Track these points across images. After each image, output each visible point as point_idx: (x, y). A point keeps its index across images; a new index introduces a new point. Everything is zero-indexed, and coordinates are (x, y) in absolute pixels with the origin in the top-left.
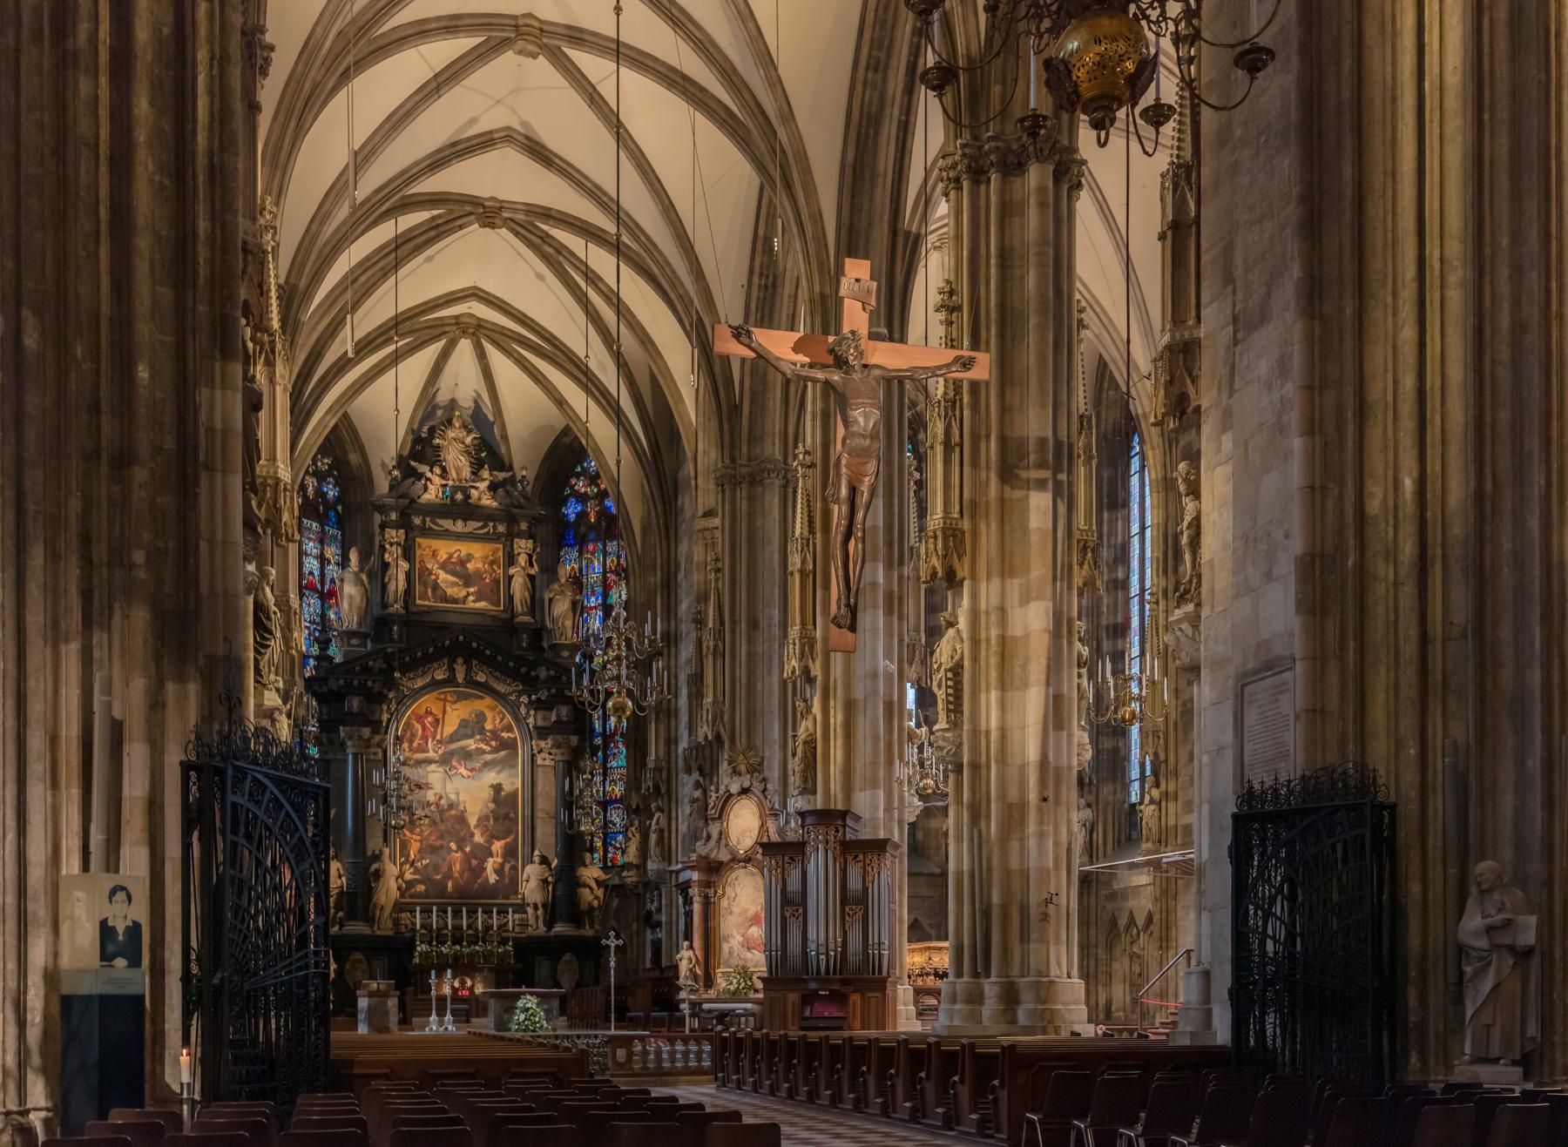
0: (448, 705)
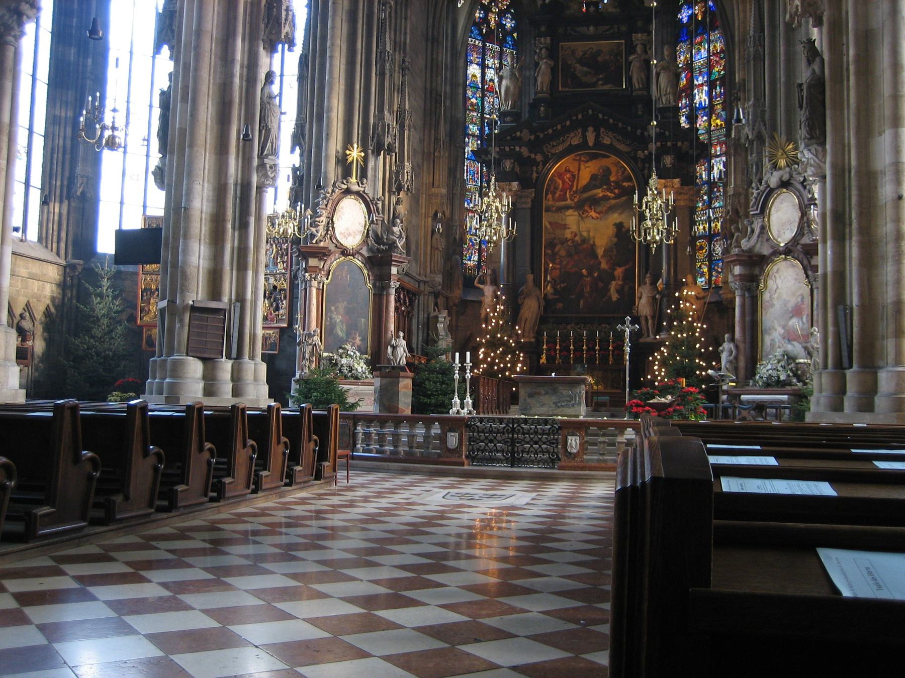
0: (582, 163)
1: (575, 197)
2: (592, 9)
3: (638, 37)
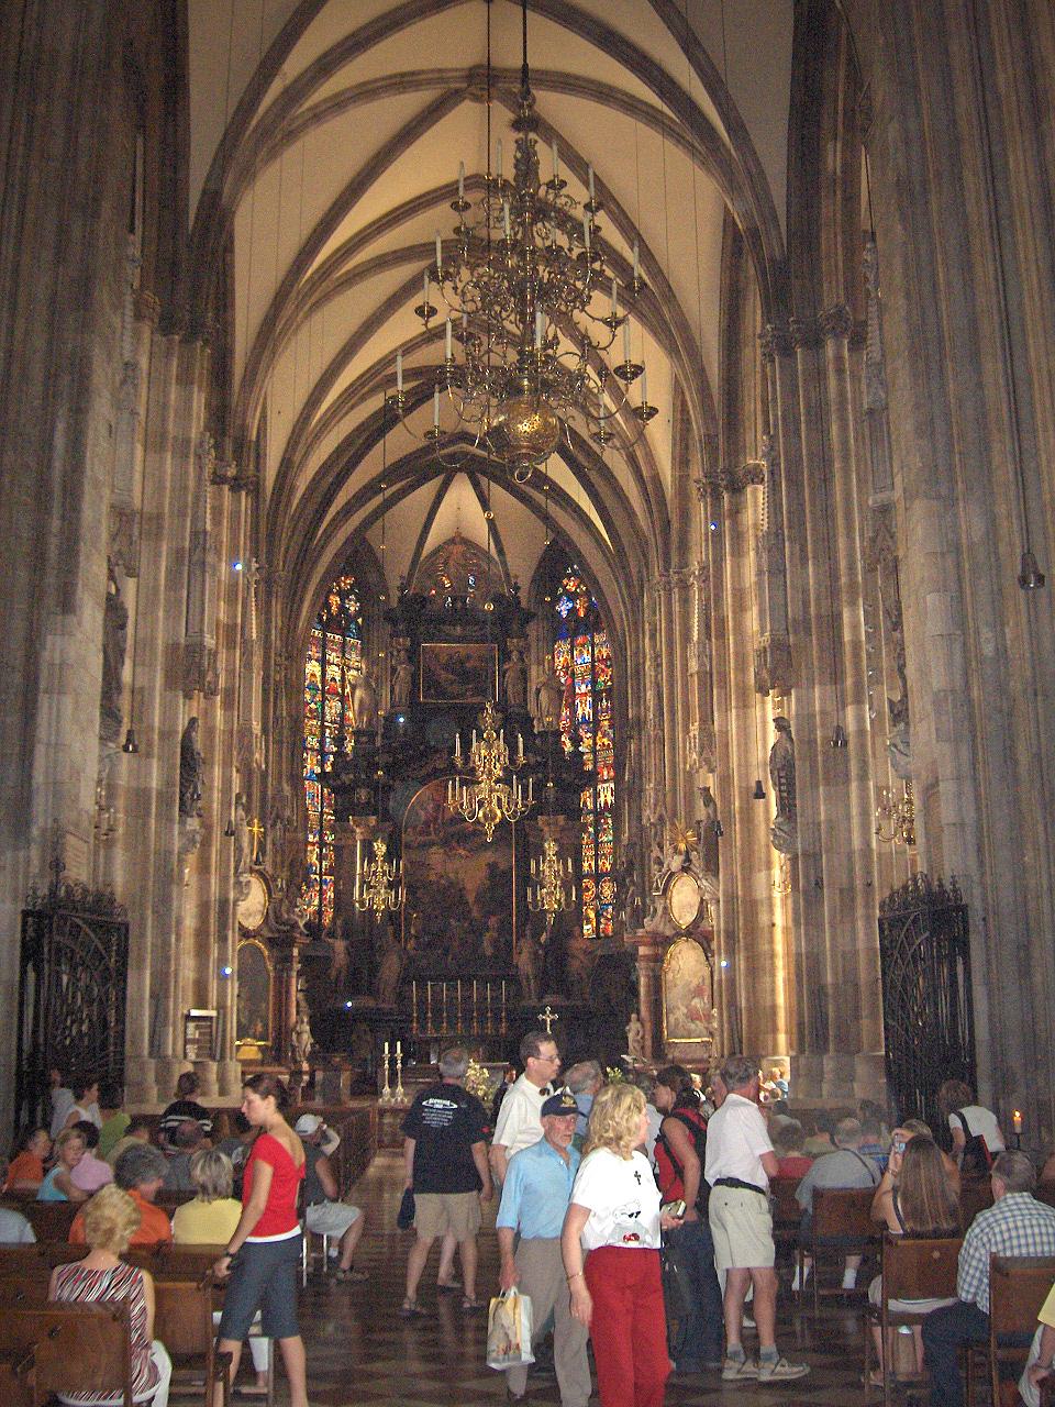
2: (459, 605)
3: (513, 643)
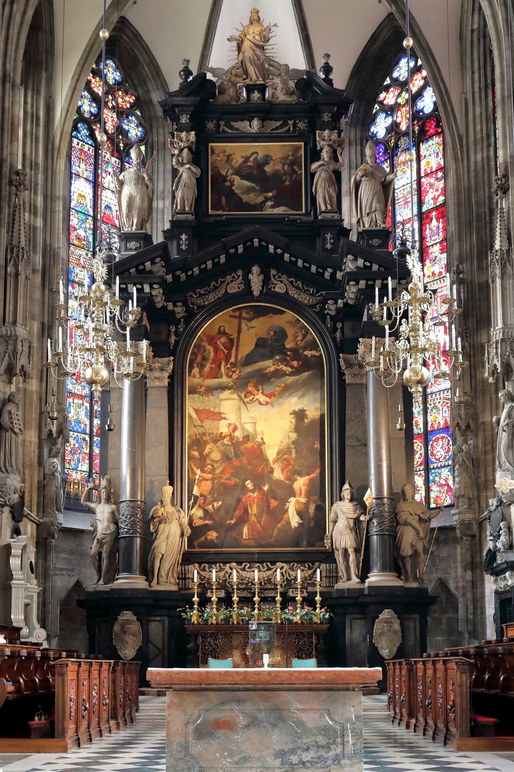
0: (243, 322)
1: (234, 372)
